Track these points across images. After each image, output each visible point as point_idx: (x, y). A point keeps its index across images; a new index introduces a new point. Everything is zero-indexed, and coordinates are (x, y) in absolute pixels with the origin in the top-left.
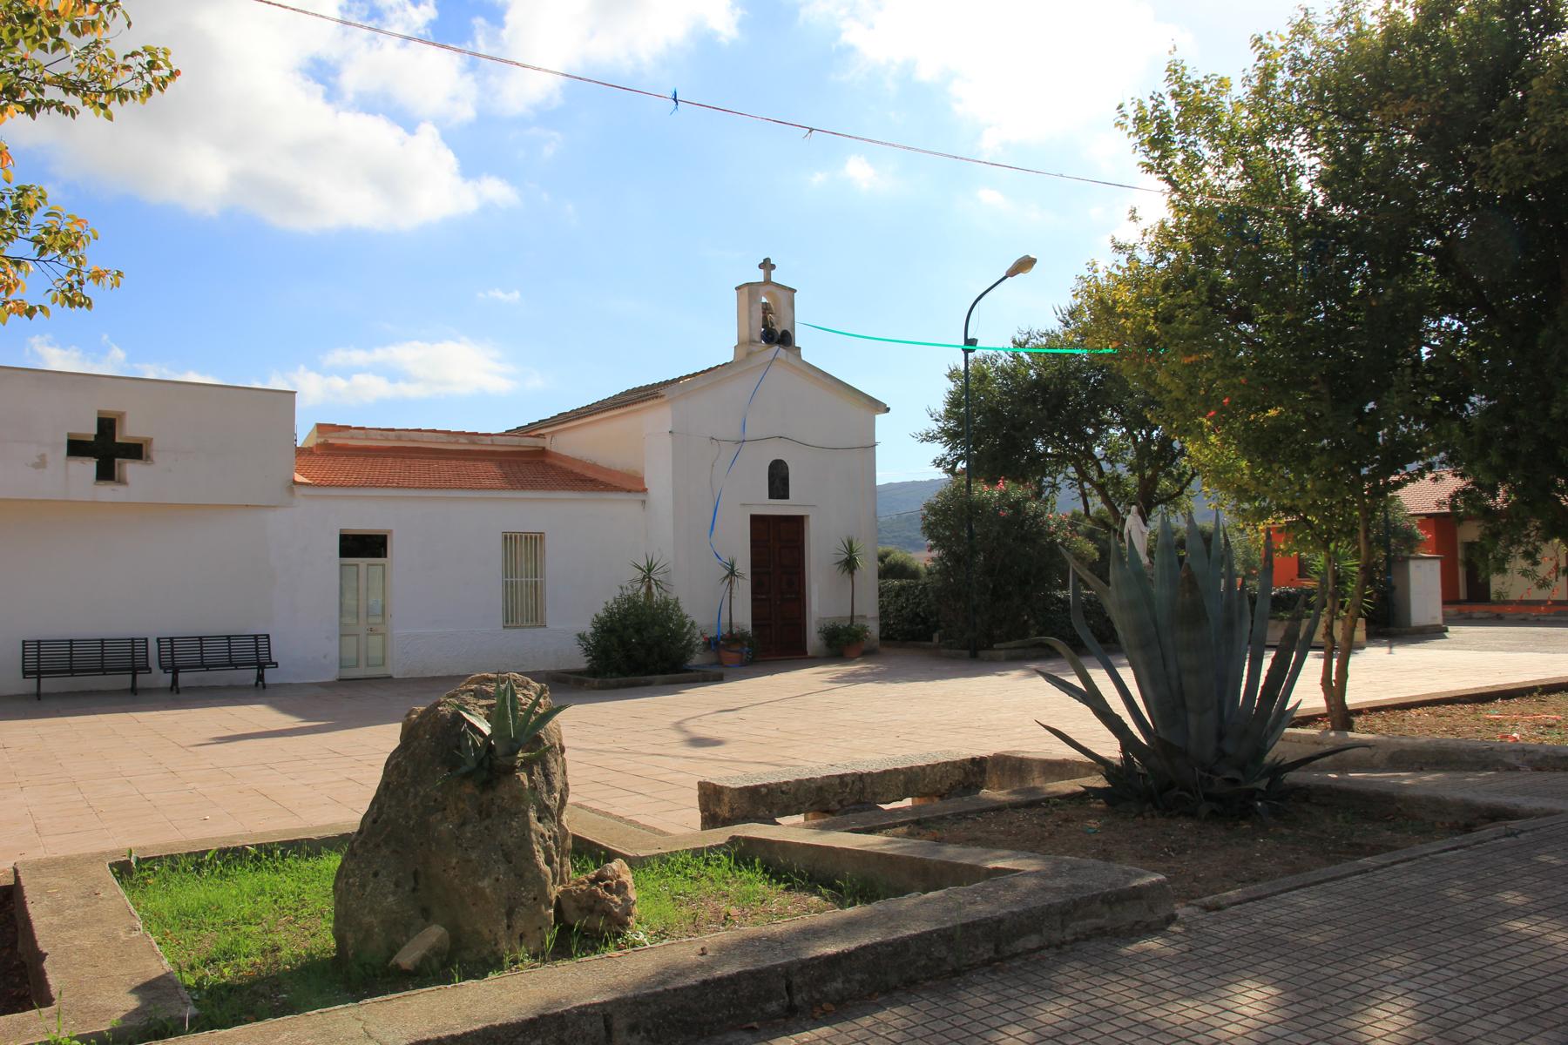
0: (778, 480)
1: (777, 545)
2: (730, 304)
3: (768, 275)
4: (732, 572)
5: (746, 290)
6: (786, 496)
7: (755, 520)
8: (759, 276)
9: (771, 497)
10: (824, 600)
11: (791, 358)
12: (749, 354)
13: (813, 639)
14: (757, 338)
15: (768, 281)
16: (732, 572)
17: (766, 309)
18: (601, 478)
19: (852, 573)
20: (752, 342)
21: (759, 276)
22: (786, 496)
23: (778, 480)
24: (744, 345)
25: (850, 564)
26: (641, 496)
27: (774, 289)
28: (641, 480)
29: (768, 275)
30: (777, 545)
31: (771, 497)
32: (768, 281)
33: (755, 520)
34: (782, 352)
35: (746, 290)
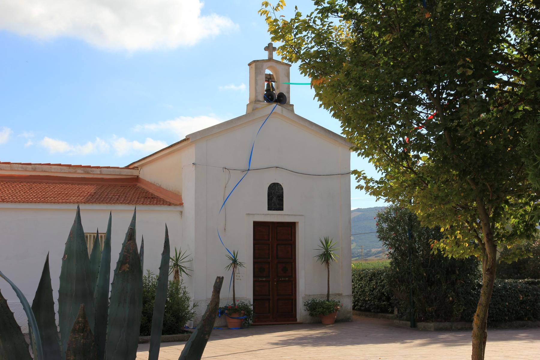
0: (275, 197)
1: (274, 244)
2: (245, 73)
3: (271, 55)
4: (235, 262)
5: (253, 65)
6: (281, 209)
7: (257, 225)
8: (265, 56)
9: (269, 209)
10: (309, 282)
11: (285, 112)
12: (254, 110)
13: (301, 311)
14: (261, 98)
15: (271, 59)
16: (235, 262)
17: (269, 78)
18: (162, 196)
19: (327, 263)
20: (257, 101)
21: (265, 56)
22: (281, 209)
23: (275, 197)
24: (253, 104)
25: (326, 257)
26: (179, 208)
27: (274, 64)
28: (181, 199)
29: (271, 55)
30: (274, 244)
31: (269, 209)
32: (271, 59)
33: (257, 225)
34: (278, 108)
35: (253, 65)
